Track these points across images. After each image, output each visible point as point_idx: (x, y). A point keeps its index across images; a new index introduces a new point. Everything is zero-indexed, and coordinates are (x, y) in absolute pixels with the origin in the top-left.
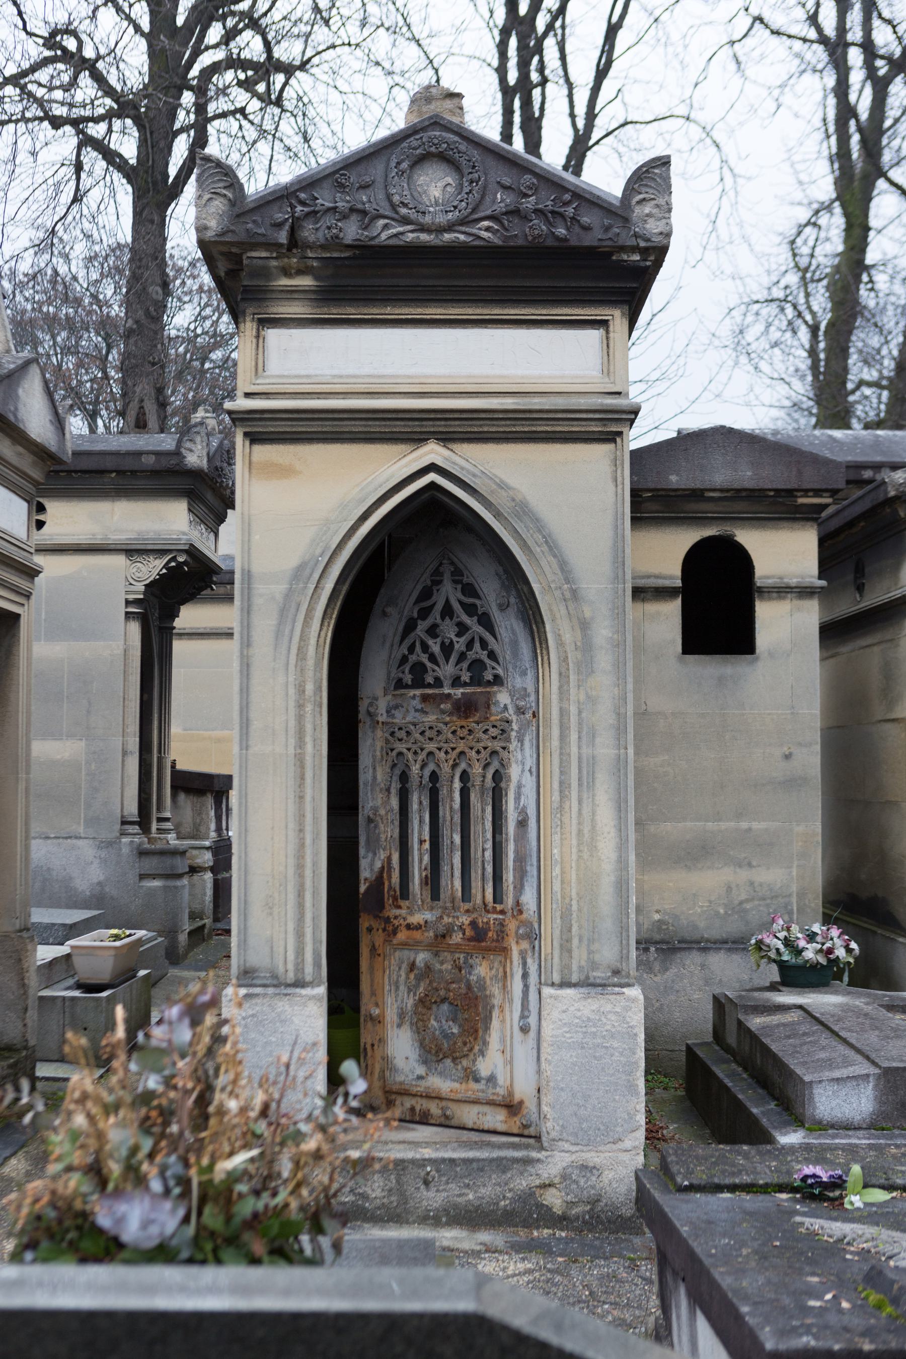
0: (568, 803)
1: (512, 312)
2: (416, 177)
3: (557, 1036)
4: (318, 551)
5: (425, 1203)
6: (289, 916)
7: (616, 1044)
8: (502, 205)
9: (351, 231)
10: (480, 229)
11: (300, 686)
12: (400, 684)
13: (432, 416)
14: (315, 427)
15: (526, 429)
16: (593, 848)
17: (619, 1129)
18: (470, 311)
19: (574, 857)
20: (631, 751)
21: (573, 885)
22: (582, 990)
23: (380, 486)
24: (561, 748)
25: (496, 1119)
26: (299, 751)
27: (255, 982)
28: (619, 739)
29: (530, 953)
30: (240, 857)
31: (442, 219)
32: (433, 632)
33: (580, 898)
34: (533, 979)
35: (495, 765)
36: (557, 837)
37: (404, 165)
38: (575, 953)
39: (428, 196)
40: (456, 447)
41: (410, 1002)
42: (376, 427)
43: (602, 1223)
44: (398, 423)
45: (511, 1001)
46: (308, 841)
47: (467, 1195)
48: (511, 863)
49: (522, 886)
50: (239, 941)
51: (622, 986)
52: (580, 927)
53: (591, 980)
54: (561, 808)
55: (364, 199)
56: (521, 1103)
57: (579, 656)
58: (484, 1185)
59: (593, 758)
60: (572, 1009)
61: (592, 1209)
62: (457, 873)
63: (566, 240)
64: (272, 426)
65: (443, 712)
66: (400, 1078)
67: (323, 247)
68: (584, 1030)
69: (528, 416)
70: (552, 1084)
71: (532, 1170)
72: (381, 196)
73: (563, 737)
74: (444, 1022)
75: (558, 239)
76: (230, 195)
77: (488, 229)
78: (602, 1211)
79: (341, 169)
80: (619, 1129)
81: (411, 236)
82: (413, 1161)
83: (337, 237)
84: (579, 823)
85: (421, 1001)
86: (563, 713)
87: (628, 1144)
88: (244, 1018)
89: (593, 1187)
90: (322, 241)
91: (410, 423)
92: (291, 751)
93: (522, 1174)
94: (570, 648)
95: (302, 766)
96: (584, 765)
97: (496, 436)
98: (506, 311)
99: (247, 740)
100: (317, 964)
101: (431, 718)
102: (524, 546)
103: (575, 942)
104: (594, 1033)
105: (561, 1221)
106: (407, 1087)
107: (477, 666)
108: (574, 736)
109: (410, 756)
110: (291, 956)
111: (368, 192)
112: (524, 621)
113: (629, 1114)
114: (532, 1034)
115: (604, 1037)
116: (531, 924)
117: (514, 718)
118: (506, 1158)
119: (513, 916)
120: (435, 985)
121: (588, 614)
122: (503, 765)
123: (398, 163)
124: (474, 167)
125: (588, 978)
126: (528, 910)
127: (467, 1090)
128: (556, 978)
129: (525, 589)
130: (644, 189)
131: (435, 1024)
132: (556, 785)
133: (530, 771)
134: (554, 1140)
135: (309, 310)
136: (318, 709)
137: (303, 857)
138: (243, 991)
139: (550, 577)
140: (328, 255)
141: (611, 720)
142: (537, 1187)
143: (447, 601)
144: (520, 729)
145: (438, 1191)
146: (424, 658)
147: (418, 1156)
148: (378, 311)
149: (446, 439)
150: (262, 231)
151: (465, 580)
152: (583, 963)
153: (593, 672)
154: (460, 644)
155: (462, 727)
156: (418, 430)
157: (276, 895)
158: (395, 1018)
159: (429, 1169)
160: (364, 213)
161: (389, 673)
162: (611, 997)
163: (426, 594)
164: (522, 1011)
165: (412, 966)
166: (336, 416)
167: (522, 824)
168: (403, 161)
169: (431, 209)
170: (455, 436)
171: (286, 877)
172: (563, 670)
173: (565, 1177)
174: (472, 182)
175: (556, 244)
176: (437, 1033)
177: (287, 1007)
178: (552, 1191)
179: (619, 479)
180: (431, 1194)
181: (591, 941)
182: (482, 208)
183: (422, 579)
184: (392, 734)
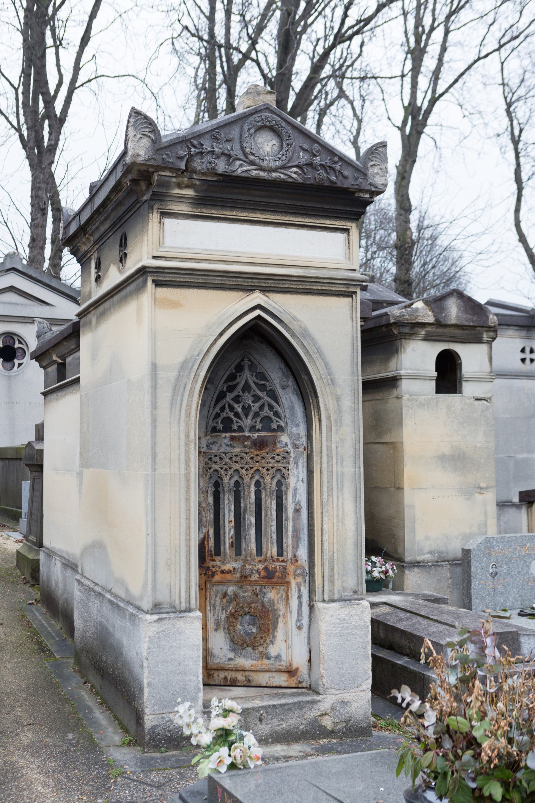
1: (301, 220)
2: (256, 138)
8: (303, 160)
9: (221, 166)
10: (291, 172)
12: (214, 430)
13: (259, 277)
14: (193, 279)
15: (295, 287)
18: (278, 218)
23: (230, 316)
25: (282, 679)
29: (303, 584)
31: (273, 165)
32: (237, 399)
35: (278, 477)
37: (252, 131)
39: (263, 150)
40: (270, 295)
41: (223, 616)
42: (227, 281)
44: (240, 280)
45: (291, 612)
48: (290, 533)
49: (298, 546)
55: (229, 148)
56: (297, 669)
62: (253, 539)
63: (335, 183)
64: (169, 277)
65: (245, 446)
66: (216, 661)
67: (203, 174)
69: (309, 280)
72: (237, 147)
74: (246, 626)
75: (331, 182)
76: (152, 137)
77: (295, 173)
79: (216, 129)
81: (254, 173)
83: (214, 169)
85: (232, 615)
90: (205, 170)
91: (246, 280)
97: (291, 290)
98: (297, 219)
101: (237, 450)
102: (307, 352)
106: (222, 666)
107: (267, 420)
109: (223, 472)
111: (231, 144)
116: (304, 567)
119: (292, 563)
120: (241, 605)
122: (284, 477)
123: (249, 129)
124: (289, 136)
126: (301, 559)
127: (262, 665)
130: (374, 159)
131: (240, 627)
133: (302, 480)
135: (189, 209)
140: (205, 178)
143: (246, 381)
144: (296, 457)
146: (231, 415)
148: (228, 213)
149: (265, 290)
150: (171, 160)
151: (258, 370)
154: (255, 407)
155: (257, 455)
156: (250, 284)
158: (213, 626)
160: (229, 156)
161: (207, 423)
163: (232, 377)
164: (298, 617)
165: (225, 595)
166: (206, 273)
168: (251, 128)
169: (267, 158)
170: (270, 289)
174: (288, 145)
175: (330, 185)
176: (242, 632)
179: (354, 318)
182: (292, 160)
183: (230, 369)
184: (210, 459)
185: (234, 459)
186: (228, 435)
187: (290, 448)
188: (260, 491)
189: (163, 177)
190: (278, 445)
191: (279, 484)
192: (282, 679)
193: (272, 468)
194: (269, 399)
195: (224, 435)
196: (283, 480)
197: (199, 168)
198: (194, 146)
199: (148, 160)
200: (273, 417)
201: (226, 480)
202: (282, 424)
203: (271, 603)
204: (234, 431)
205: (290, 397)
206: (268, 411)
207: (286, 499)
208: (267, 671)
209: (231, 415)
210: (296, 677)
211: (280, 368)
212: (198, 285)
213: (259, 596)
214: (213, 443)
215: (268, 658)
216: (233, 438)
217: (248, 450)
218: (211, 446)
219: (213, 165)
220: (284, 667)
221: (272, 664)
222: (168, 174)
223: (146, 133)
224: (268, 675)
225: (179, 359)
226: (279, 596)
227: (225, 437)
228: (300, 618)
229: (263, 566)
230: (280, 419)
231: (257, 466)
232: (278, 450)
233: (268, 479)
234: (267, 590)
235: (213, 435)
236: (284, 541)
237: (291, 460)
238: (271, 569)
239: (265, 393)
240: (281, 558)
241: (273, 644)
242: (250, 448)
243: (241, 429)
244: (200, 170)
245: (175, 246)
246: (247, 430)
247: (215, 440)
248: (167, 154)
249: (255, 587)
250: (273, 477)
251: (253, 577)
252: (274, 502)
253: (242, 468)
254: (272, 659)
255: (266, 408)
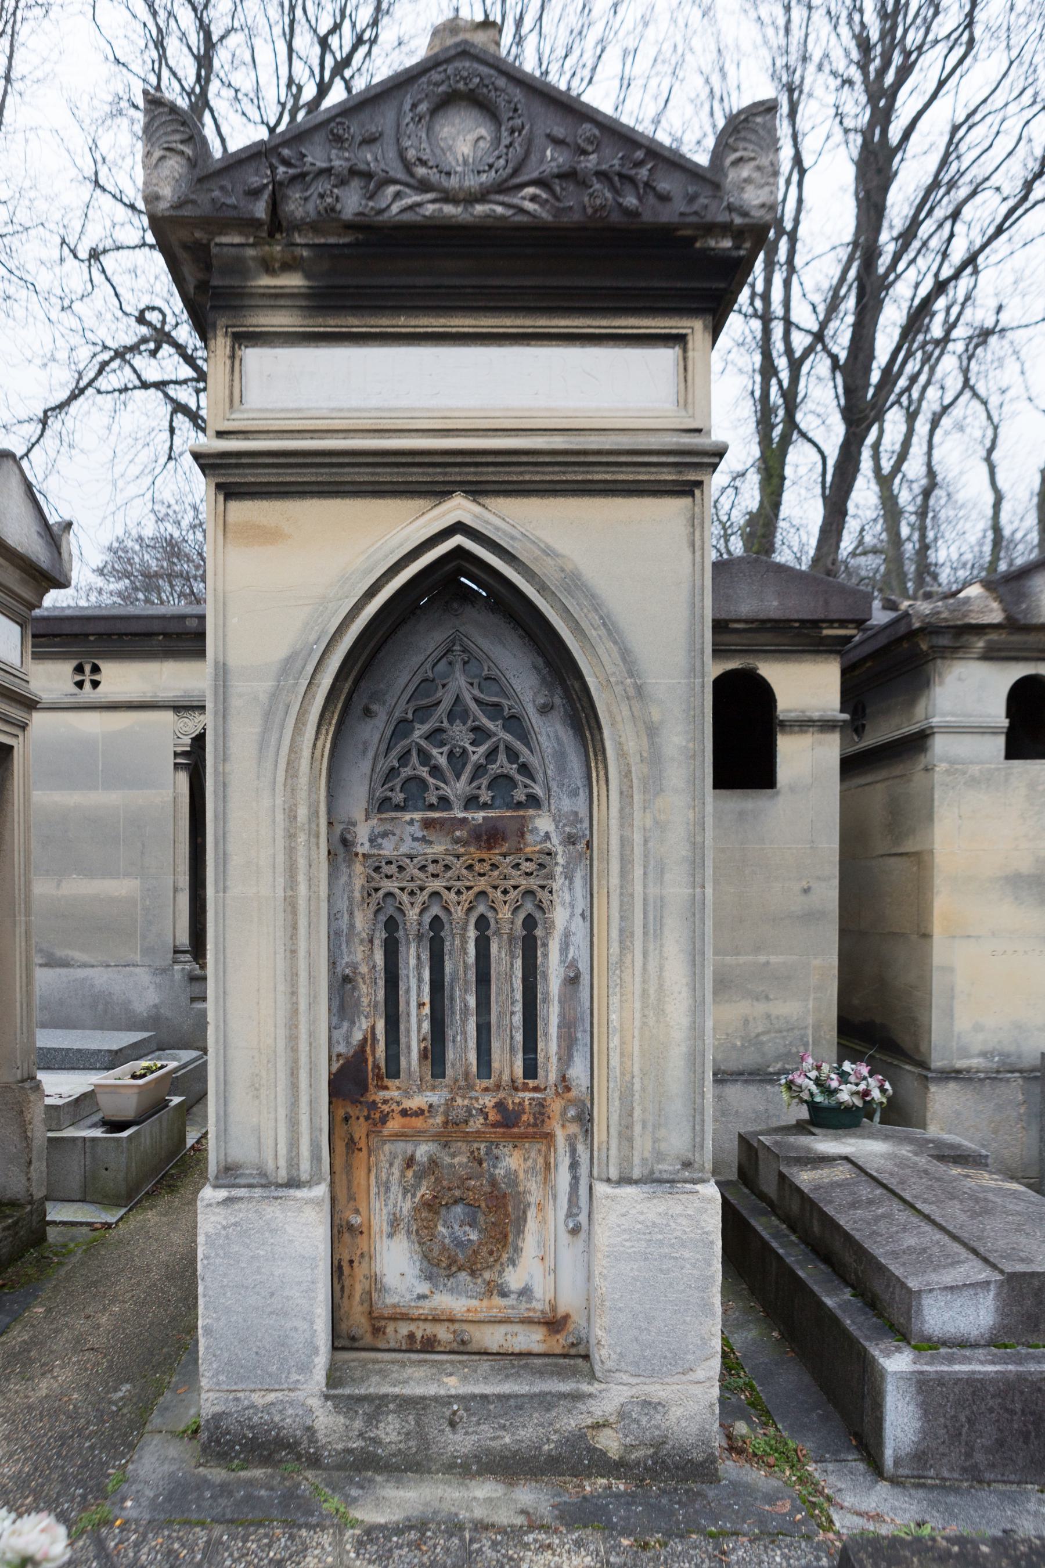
0: (629, 957)
2: (437, 128)
3: (615, 1246)
4: (313, 637)
5: (451, 1448)
6: (279, 1099)
7: (687, 1254)
8: (553, 164)
10: (523, 198)
11: (291, 810)
13: (459, 460)
16: (660, 1011)
17: (690, 1357)
18: (508, 322)
19: (637, 1024)
20: (709, 890)
21: (636, 1059)
22: (646, 1188)
24: (622, 887)
26: (290, 893)
27: (238, 1181)
28: (694, 876)
29: (580, 1138)
30: (217, 1027)
31: (472, 182)
33: (644, 1073)
34: (583, 1171)
36: (615, 1000)
37: (423, 107)
38: (638, 1143)
42: (386, 475)
43: (668, 1469)
44: (415, 470)
46: (303, 1006)
47: (503, 1438)
49: (570, 1057)
50: (218, 1131)
51: (694, 1182)
52: (644, 1110)
53: (657, 1175)
54: (621, 962)
55: (369, 157)
56: (566, 1317)
57: (646, 770)
58: (524, 1426)
59: (662, 898)
60: (633, 1211)
61: (655, 1453)
68: (648, 1237)
69: (582, 459)
70: (607, 1304)
71: (583, 1408)
72: (392, 154)
73: (625, 873)
77: (533, 199)
78: (668, 1455)
80: (690, 1357)
81: (430, 209)
82: (436, 1399)
83: (333, 210)
84: (644, 982)
86: (625, 843)
87: (700, 1374)
88: (224, 1228)
89: (658, 1427)
91: (430, 470)
92: (280, 893)
93: (569, 1411)
94: (634, 760)
95: (294, 913)
96: (651, 908)
99: (224, 881)
100: (316, 1157)
103: (638, 1129)
104: (660, 1241)
105: (617, 1468)
108: (638, 872)
110: (282, 1150)
112: (573, 727)
113: (702, 1339)
114: (583, 1235)
115: (672, 1246)
117: (560, 849)
118: (550, 1393)
121: (656, 717)
123: (414, 106)
125: (652, 1172)
128: (614, 1174)
129: (577, 685)
132: (615, 934)
133: (583, 915)
134: (610, 1371)
135: (298, 321)
136: (313, 840)
137: (296, 1027)
138: (223, 1194)
139: (610, 668)
140: (322, 241)
141: (683, 850)
142: (588, 1427)
144: (568, 863)
145: (466, 1433)
147: (442, 1392)
149: (476, 491)
152: (647, 1155)
153: (662, 790)
157: (264, 1074)
159: (455, 1407)
160: (368, 176)
162: (681, 1197)
164: (569, 1208)
167: (572, 981)
168: (420, 101)
169: (459, 169)
171: (275, 1052)
172: (625, 788)
173: (622, 1415)
174: (512, 132)
177: (278, 1214)
178: (608, 1432)
180: (459, 1437)
181: (657, 1126)
185: (431, 868)
186: (417, 816)
187: (556, 843)
188: (488, 939)
189: (225, 249)
190: (529, 838)
191: (530, 923)
192: (532, 1339)
193: (515, 887)
194: (508, 737)
195: (408, 816)
196: (538, 915)
197: (299, 213)
198: (286, 163)
199: (179, 205)
200: (518, 777)
201: (413, 914)
202: (538, 790)
203: (512, 1179)
204: (431, 807)
205: (556, 732)
206: (505, 763)
207: (546, 955)
208: (500, 1322)
209: (424, 772)
210: (564, 1333)
211: (535, 667)
212: (321, 488)
213: (485, 1165)
214: (385, 835)
215: (504, 1294)
216: (427, 824)
217: (462, 850)
218: (380, 840)
219: (329, 200)
220: (538, 1314)
221: (513, 1307)
222: (237, 240)
223: (174, 145)
224: (502, 1329)
225: (281, 652)
226: (529, 1163)
227: (411, 822)
228: (575, 1211)
229: (494, 1100)
230: (534, 780)
231: (482, 884)
232: (528, 850)
233: (505, 913)
234: (502, 1151)
235: (383, 816)
236: (541, 1045)
237: (559, 869)
238: (511, 1107)
239: (500, 722)
240: (531, 1083)
241: (514, 1265)
242: (466, 843)
243: (444, 803)
244: (302, 219)
245: (270, 406)
246: (457, 804)
247: (388, 827)
248: (222, 188)
249: (476, 1145)
250: (517, 908)
251: (471, 1123)
252: (518, 963)
253: (449, 889)
254: (513, 1296)
255: (502, 757)
